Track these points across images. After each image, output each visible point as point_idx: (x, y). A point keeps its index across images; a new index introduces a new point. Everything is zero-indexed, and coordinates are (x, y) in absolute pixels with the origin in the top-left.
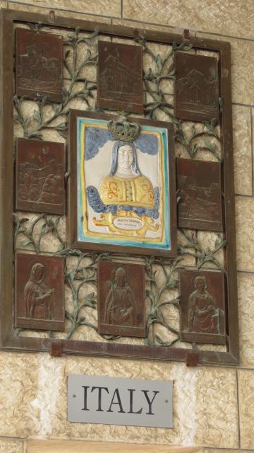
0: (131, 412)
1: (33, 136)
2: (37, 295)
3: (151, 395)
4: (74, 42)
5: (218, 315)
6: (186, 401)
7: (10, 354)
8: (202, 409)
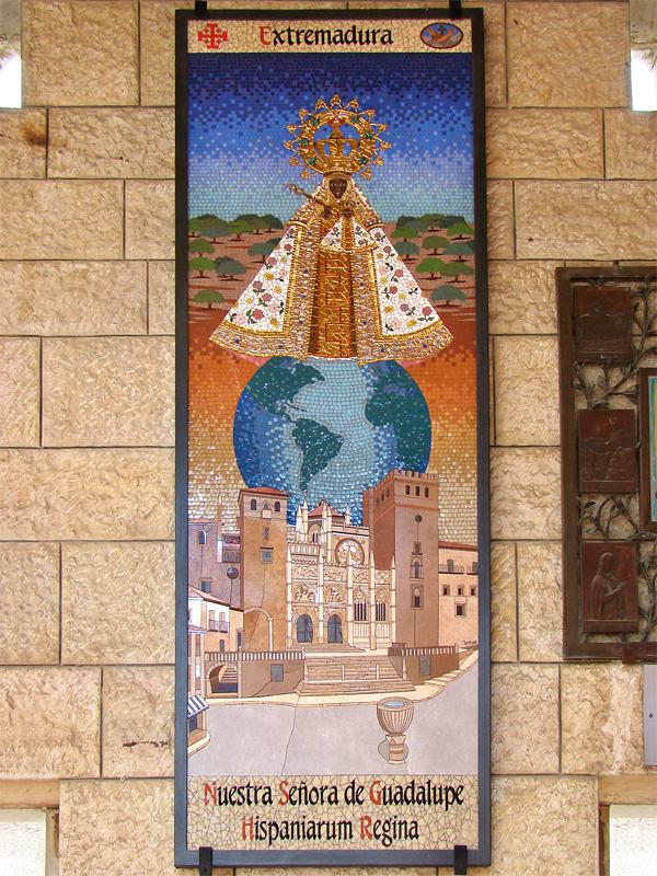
1: (598, 406)
4: (644, 293)
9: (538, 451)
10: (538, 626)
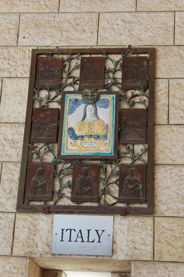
0: (88, 241)
1: (43, 107)
2: (38, 183)
3: (100, 233)
4: (70, 60)
5: (141, 188)
6: (121, 235)
7: (24, 214)
8: (131, 239)
9: (17, 125)
10: (7, 197)
